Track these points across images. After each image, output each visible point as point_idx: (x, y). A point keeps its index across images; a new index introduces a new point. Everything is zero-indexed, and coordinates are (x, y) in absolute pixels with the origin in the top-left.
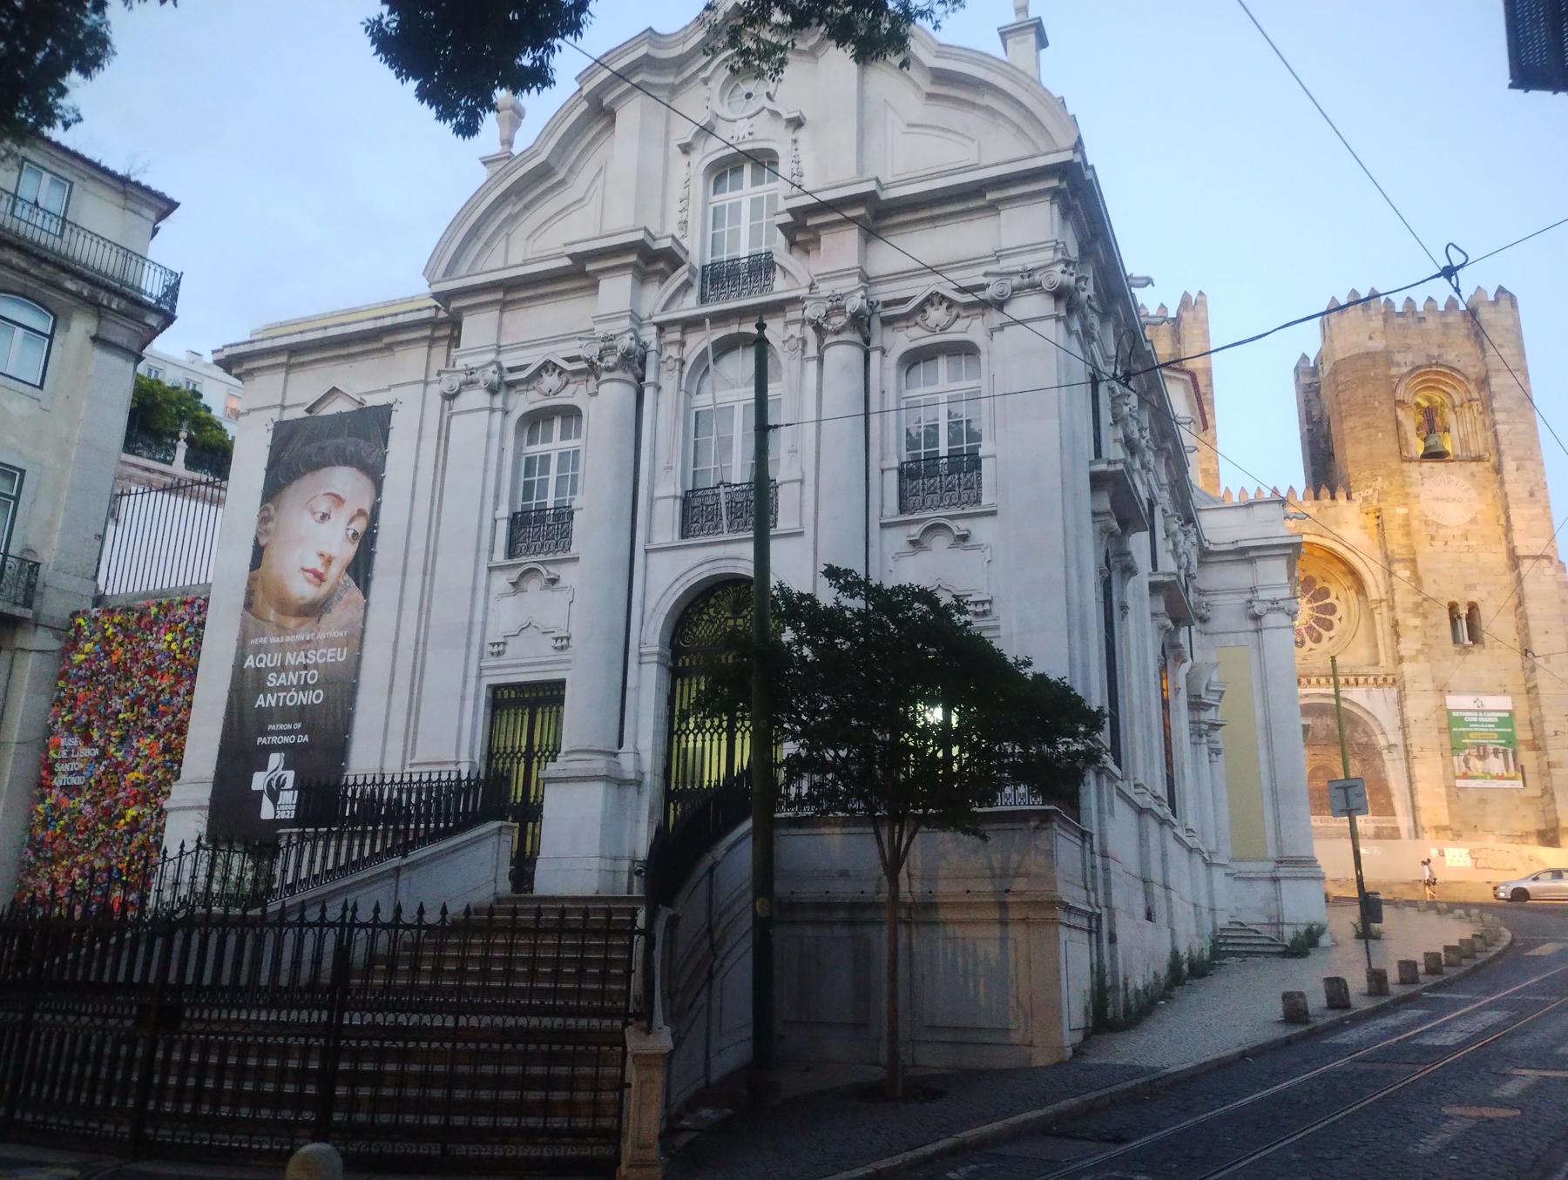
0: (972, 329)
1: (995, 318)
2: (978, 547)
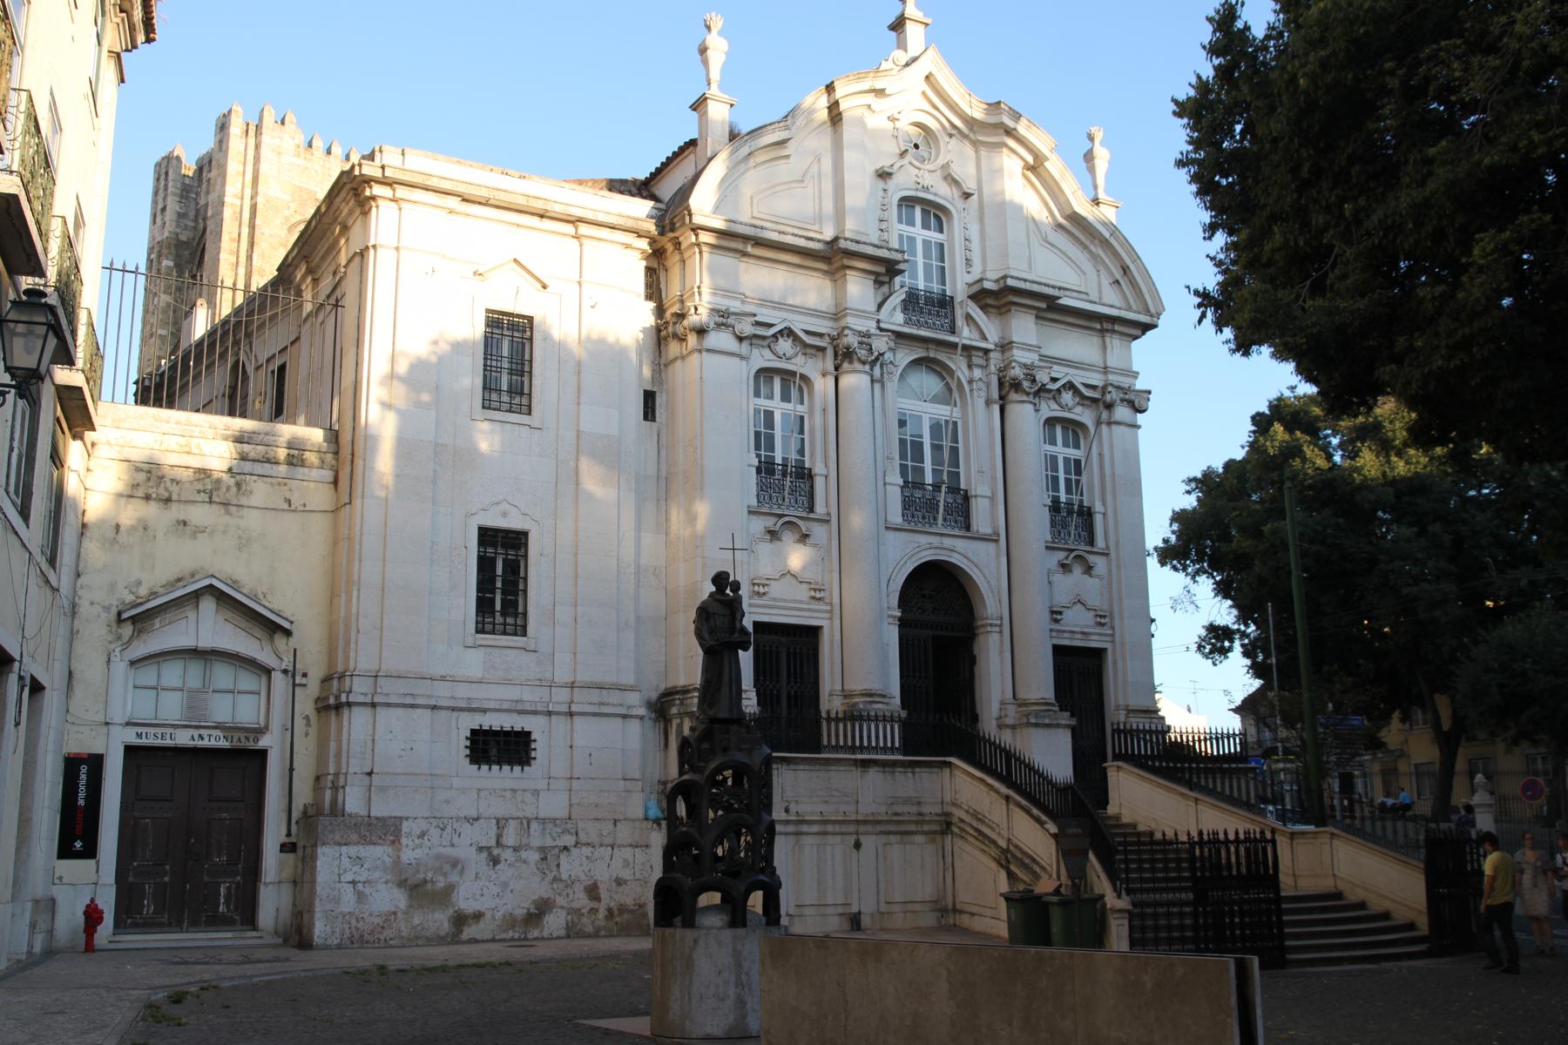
0: (1085, 416)
1: (1105, 415)
2: (1098, 577)
